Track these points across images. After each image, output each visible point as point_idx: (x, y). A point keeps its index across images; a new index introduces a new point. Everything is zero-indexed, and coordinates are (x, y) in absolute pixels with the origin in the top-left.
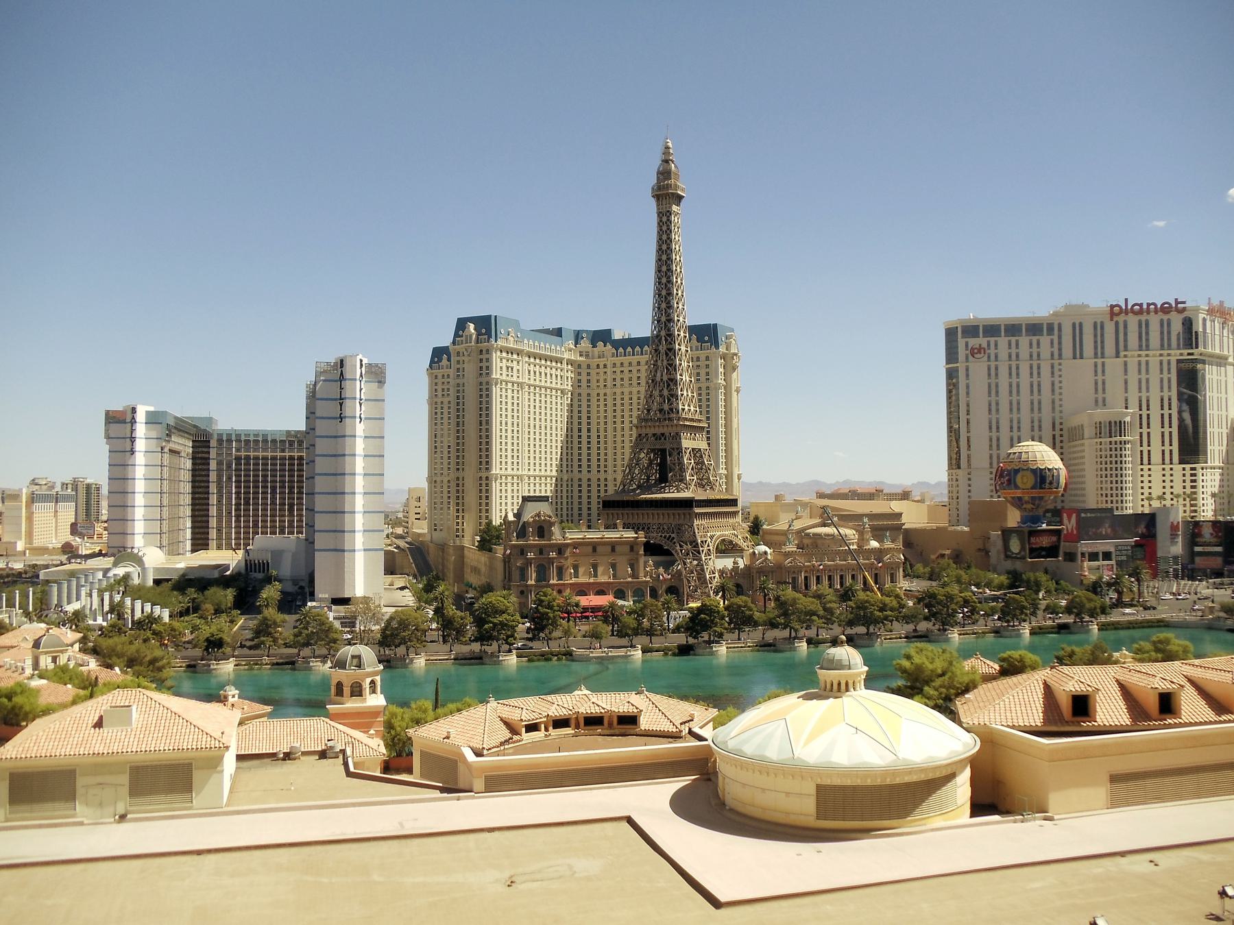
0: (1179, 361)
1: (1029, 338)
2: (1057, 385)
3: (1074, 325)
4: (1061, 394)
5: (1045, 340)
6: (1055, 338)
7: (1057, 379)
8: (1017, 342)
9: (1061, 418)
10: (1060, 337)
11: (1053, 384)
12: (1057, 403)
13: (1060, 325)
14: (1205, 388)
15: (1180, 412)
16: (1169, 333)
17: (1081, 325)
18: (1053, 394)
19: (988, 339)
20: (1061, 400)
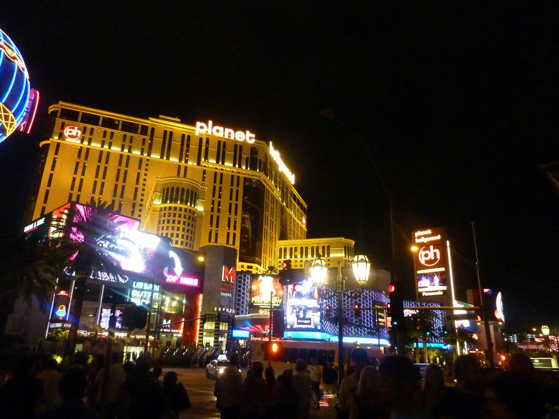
0: (245, 178)
1: (123, 133)
2: (142, 177)
3: (165, 132)
4: (144, 185)
5: (138, 137)
6: (148, 137)
7: (143, 172)
8: (112, 133)
9: (141, 205)
10: (151, 139)
11: (139, 174)
12: (140, 192)
13: (153, 129)
14: (263, 207)
15: (243, 219)
16: (240, 156)
17: (171, 133)
18: (137, 182)
19: (86, 125)
20: (143, 190)
